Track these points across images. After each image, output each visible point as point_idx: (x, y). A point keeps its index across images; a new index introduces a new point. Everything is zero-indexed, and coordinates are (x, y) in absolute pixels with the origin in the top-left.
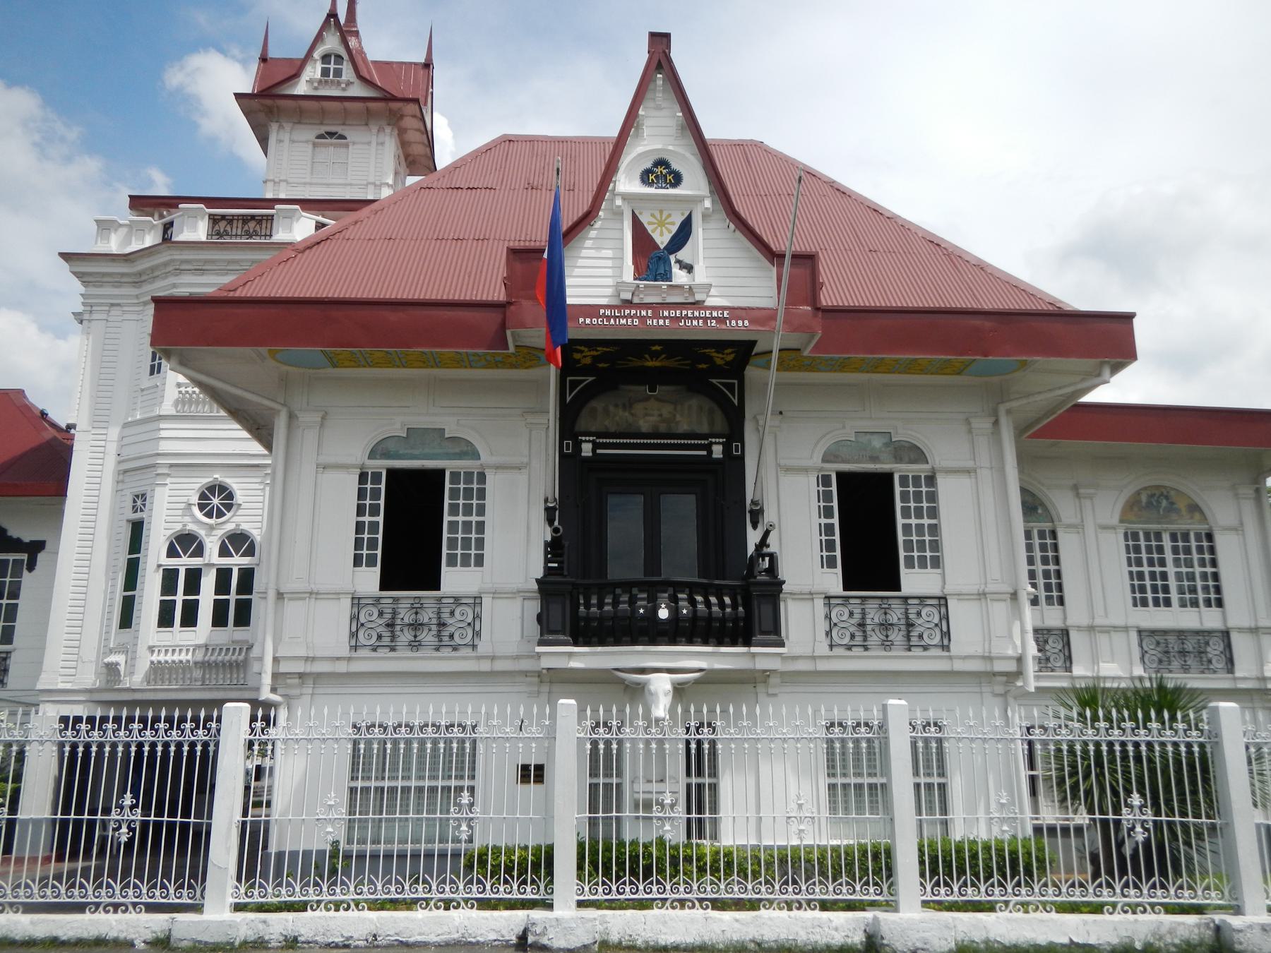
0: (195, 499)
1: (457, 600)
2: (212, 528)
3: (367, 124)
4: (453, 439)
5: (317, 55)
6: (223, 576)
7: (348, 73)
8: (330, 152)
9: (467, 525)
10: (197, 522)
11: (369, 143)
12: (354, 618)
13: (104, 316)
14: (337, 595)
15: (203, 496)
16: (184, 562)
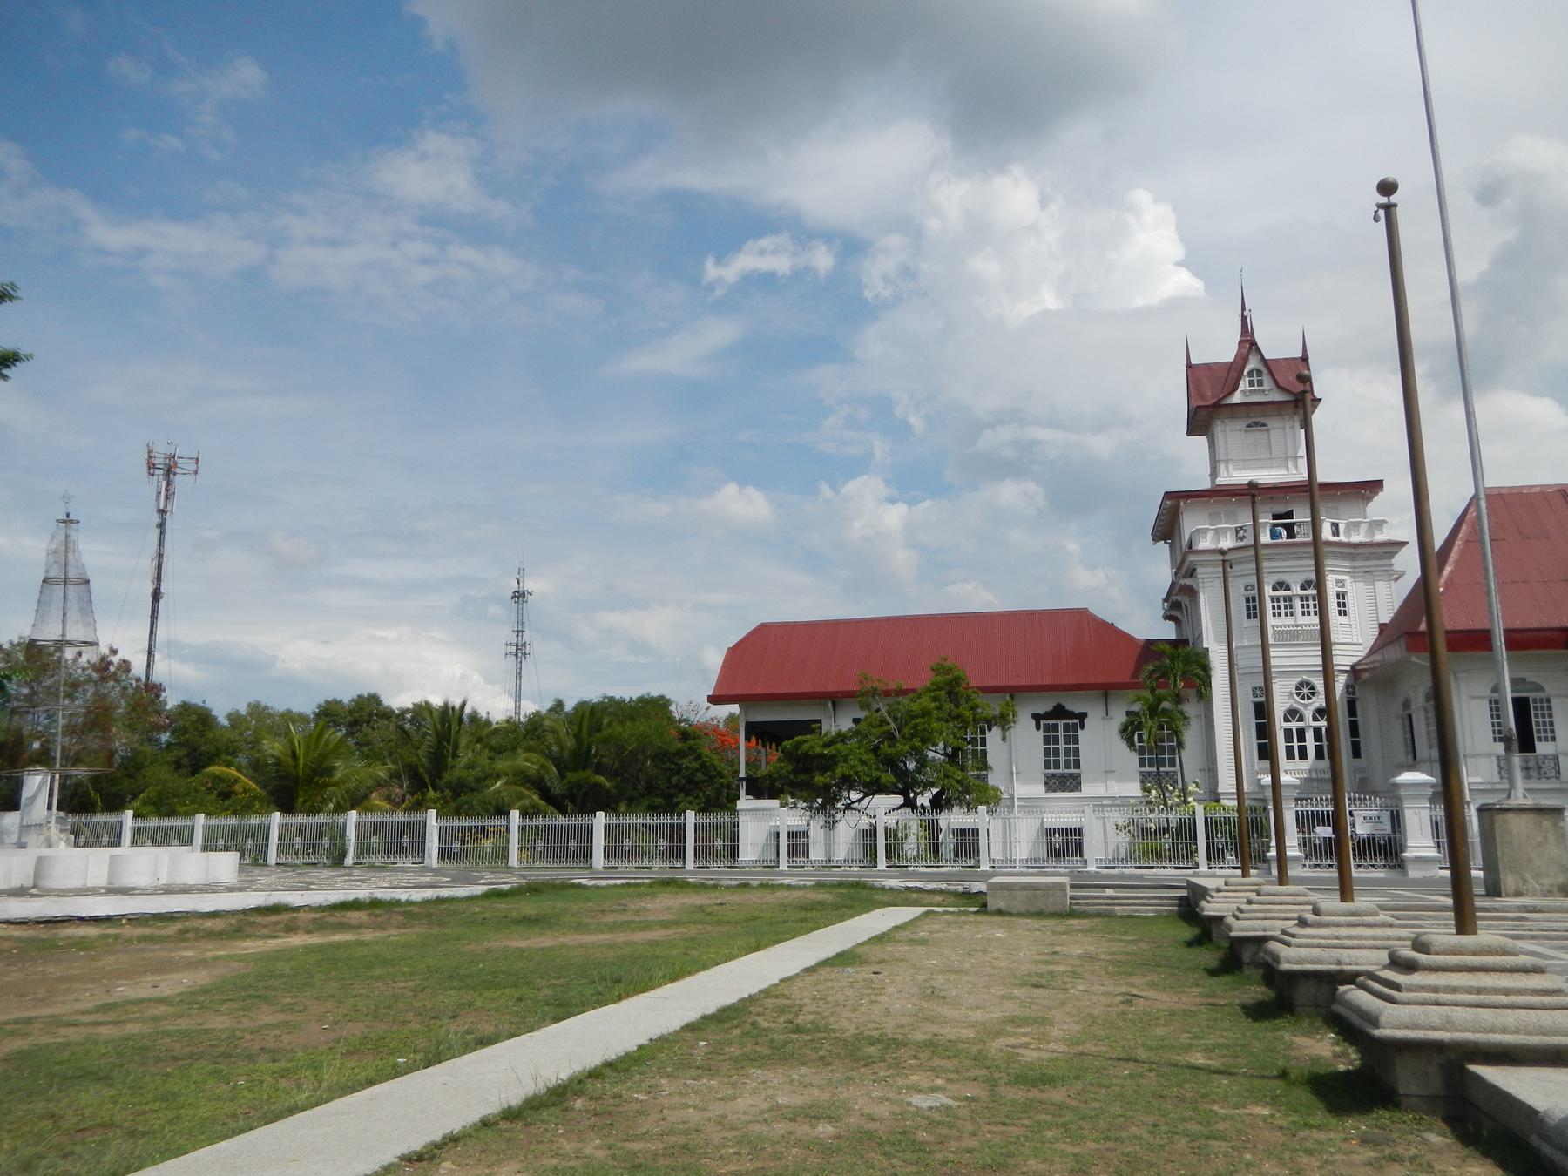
0: (1294, 691)
1: (1545, 757)
2: (1306, 706)
3: (1280, 415)
4: (1531, 683)
5: (1245, 373)
6: (1317, 732)
7: (1268, 383)
8: (1258, 436)
9: (1544, 724)
10: (1297, 703)
11: (1284, 428)
12: (1499, 765)
13: (1210, 584)
14: (1489, 755)
15: (1297, 688)
16: (1294, 725)
